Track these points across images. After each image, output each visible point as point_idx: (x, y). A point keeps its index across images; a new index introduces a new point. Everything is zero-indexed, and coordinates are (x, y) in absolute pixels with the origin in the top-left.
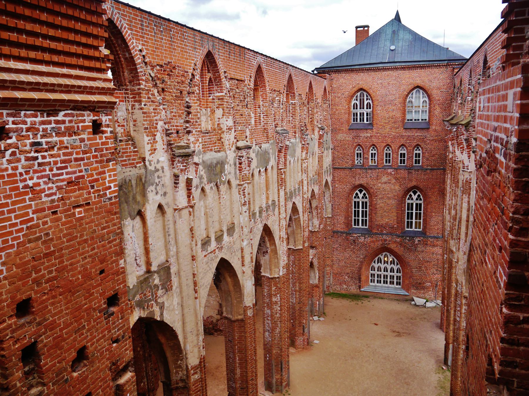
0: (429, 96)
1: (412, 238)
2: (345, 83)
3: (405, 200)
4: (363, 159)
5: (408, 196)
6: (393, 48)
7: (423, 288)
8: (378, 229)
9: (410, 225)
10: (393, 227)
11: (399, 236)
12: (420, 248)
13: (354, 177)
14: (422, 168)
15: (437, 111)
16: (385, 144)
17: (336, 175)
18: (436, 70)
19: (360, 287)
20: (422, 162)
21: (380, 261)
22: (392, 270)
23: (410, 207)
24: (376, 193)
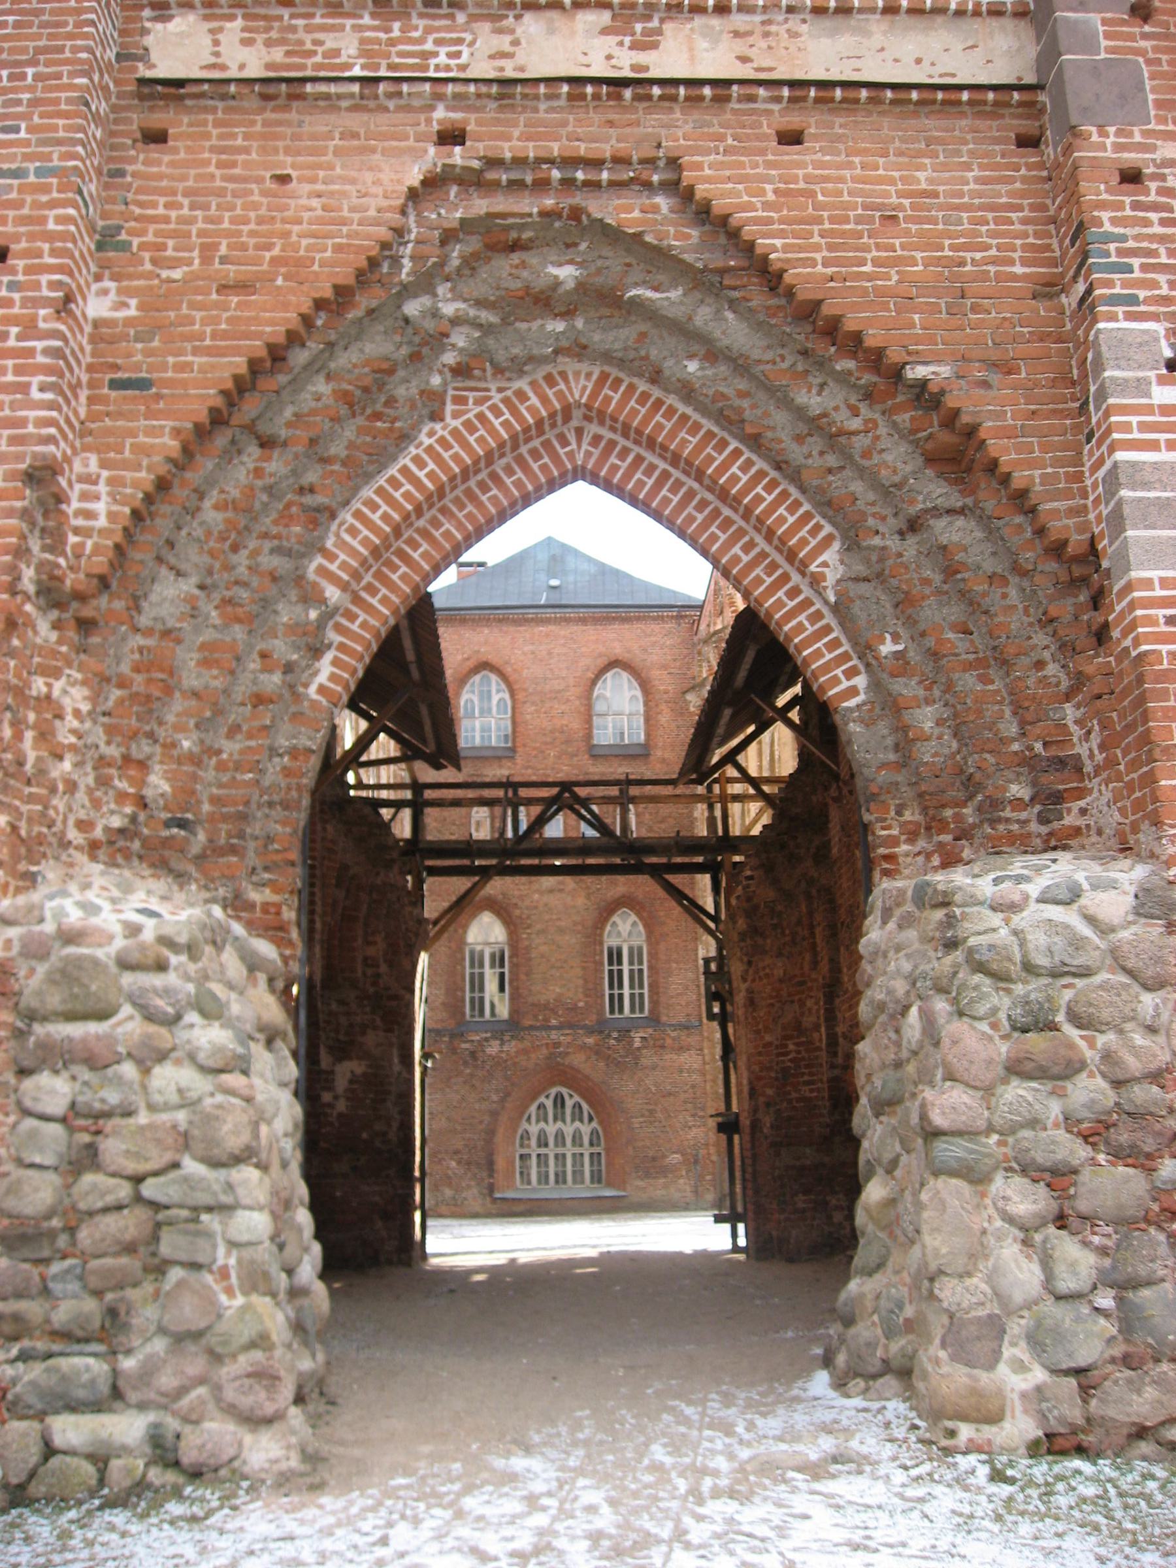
0: (645, 686)
1: (625, 1033)
6: (554, 582)
7: (664, 1171)
8: (535, 1017)
9: (616, 1002)
10: (574, 1008)
11: (590, 1031)
12: (648, 1058)
15: (665, 717)
18: (655, 627)
19: (491, 1189)
22: (577, 1139)
23: (615, 956)
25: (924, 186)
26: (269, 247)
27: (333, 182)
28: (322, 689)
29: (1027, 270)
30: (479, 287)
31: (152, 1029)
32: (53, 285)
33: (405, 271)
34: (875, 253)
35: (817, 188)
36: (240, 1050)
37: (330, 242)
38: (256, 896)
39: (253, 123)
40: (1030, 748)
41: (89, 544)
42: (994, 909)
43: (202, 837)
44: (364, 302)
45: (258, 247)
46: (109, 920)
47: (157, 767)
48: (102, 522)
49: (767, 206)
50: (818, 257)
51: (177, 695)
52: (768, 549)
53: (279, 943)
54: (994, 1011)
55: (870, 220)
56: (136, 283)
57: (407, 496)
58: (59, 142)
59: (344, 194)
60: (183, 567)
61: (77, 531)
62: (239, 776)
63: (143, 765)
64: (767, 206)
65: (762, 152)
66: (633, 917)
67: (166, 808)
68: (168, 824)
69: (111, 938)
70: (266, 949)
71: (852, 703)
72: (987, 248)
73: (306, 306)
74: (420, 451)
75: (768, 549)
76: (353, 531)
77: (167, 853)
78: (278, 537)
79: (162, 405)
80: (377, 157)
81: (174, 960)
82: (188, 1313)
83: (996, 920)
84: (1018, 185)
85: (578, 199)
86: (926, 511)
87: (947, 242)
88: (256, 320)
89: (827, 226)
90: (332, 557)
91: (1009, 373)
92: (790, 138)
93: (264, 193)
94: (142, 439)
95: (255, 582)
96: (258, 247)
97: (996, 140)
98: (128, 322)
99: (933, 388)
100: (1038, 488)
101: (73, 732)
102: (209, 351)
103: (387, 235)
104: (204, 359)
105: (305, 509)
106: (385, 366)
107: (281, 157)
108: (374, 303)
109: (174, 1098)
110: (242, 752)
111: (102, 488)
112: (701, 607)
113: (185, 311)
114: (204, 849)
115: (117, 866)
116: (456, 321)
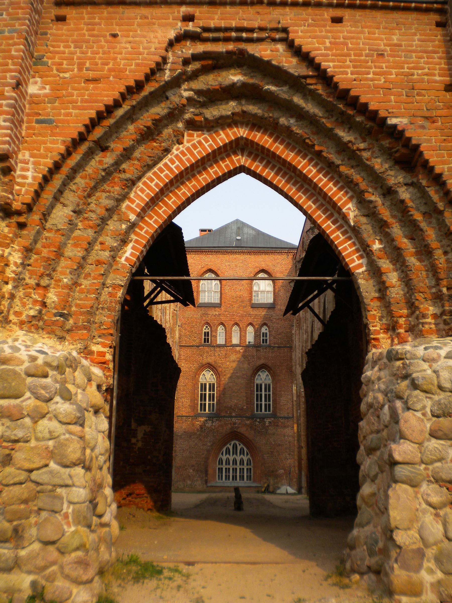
2: (195, 263)
3: (254, 379)
4: (211, 337)
5: (257, 377)
6: (239, 238)
8: (226, 412)
10: (242, 409)
11: (248, 418)
12: (271, 430)
13: (201, 356)
14: (270, 346)
16: (233, 323)
17: (182, 353)
18: (278, 257)
19: (206, 482)
20: (270, 341)
21: (228, 452)
22: (242, 462)
24: (225, 372)
25: (395, 42)
26: (107, 64)
27: (136, 37)
28: (127, 259)
29: (442, 78)
30: (199, 84)
31: (39, 403)
32: (12, 78)
33: (166, 75)
34: (374, 69)
35: (349, 41)
36: (78, 415)
37: (134, 62)
38: (95, 348)
39: (103, 13)
40: (441, 291)
41: (24, 189)
42: (424, 360)
43: (71, 321)
44: (149, 89)
45: (103, 64)
46: (23, 354)
47: (52, 290)
48: (30, 180)
49: (326, 49)
50: (349, 71)
51: (62, 258)
52: (324, 203)
53: (104, 369)
54: (424, 407)
55: (372, 56)
56: (49, 79)
57: (166, 176)
58: (19, 19)
59: (141, 42)
60: (66, 202)
61: (18, 184)
62: (89, 296)
63: (46, 288)
64: (326, 49)
65: (325, 26)
66: (267, 373)
67: (55, 308)
68: (55, 315)
69: (23, 362)
70: (97, 371)
71: (360, 270)
72: (423, 68)
73: (123, 89)
74: (173, 157)
75: (324, 203)
76: (142, 191)
77: (54, 328)
78: (109, 192)
79: (58, 130)
80: (156, 26)
81: (51, 373)
82: (50, 534)
83: (425, 366)
84: (437, 42)
85: (243, 46)
86: (395, 184)
87: (406, 66)
88: (101, 95)
89: (353, 57)
90: (133, 202)
91: (434, 122)
92: (337, 20)
93: (107, 42)
94: (49, 145)
95: (99, 210)
96: (103, 64)
97: (427, 24)
98: (46, 95)
99: (400, 128)
100: (446, 173)
101: (13, 272)
102: (79, 108)
103: (159, 60)
104: (77, 111)
105: (122, 180)
106: (157, 117)
107: (115, 26)
108: (153, 89)
109: (48, 436)
110: (90, 285)
111: (31, 166)
112: (298, 248)
113: (70, 90)
114: (72, 327)
115: (32, 332)
116: (189, 99)
